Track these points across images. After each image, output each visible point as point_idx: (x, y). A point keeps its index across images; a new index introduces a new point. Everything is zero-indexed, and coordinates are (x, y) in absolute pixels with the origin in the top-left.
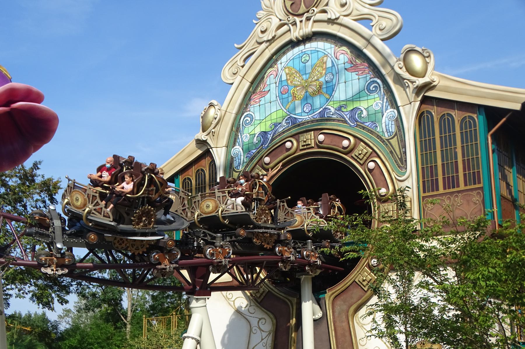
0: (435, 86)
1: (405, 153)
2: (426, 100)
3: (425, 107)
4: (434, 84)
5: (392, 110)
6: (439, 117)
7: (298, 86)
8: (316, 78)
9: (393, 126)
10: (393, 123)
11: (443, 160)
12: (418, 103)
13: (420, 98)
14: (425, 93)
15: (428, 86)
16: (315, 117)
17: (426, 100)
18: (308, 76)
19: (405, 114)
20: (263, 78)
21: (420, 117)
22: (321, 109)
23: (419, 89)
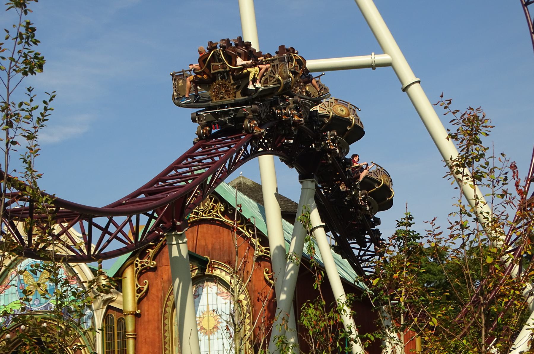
0: (114, 300)
1: (96, 340)
2: (109, 308)
3: (110, 312)
4: (114, 299)
5: (90, 311)
6: (117, 319)
7: (31, 285)
8: (43, 281)
9: (90, 322)
10: (90, 320)
11: (118, 348)
12: (104, 310)
13: (105, 307)
14: (109, 303)
15: (110, 300)
16: (42, 309)
17: (109, 308)
18: (37, 279)
19: (97, 315)
20: (7, 275)
21: (106, 317)
22: (46, 304)
23: (105, 302)
